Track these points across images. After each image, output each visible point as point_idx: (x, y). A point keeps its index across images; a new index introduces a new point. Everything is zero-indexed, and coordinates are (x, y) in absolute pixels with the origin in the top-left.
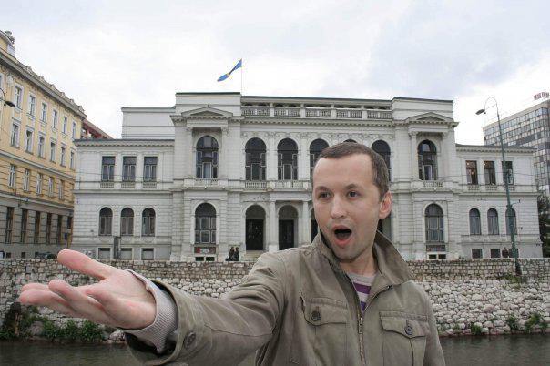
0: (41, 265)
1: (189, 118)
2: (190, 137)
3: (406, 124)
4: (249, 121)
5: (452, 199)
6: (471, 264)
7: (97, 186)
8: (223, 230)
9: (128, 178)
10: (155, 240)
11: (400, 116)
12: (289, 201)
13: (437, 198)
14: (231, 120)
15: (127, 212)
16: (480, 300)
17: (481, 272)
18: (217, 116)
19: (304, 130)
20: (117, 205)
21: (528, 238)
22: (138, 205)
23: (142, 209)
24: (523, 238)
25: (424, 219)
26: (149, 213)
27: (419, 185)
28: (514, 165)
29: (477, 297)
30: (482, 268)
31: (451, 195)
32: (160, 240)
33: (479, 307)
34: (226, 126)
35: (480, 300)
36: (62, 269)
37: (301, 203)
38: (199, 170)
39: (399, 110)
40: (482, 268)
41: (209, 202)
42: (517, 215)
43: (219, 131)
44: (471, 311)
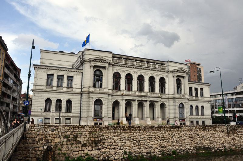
0: (59, 127)
1: (93, 61)
2: (92, 69)
3: (173, 72)
4: (115, 64)
5: (187, 102)
6: (215, 127)
7: (45, 88)
8: (106, 111)
9: (60, 85)
10: (71, 115)
11: (171, 68)
12: (130, 100)
13: (183, 101)
14: (109, 64)
15: (59, 101)
16: (219, 140)
17: (217, 130)
18: (105, 61)
19: (124, 69)
20: (54, 97)
21: (208, 117)
22: (64, 98)
23: (56, 99)
24: (206, 117)
25: (178, 108)
26: (69, 102)
27: (177, 96)
28: (204, 89)
29: (218, 139)
30: (218, 128)
31: (187, 100)
32: (74, 115)
33: (219, 142)
34: (108, 66)
35: (219, 140)
36: (70, 129)
37: (134, 100)
38: (94, 84)
39: (171, 66)
40: (218, 128)
41: (100, 99)
42: (204, 108)
43: (104, 68)
44: (217, 144)
